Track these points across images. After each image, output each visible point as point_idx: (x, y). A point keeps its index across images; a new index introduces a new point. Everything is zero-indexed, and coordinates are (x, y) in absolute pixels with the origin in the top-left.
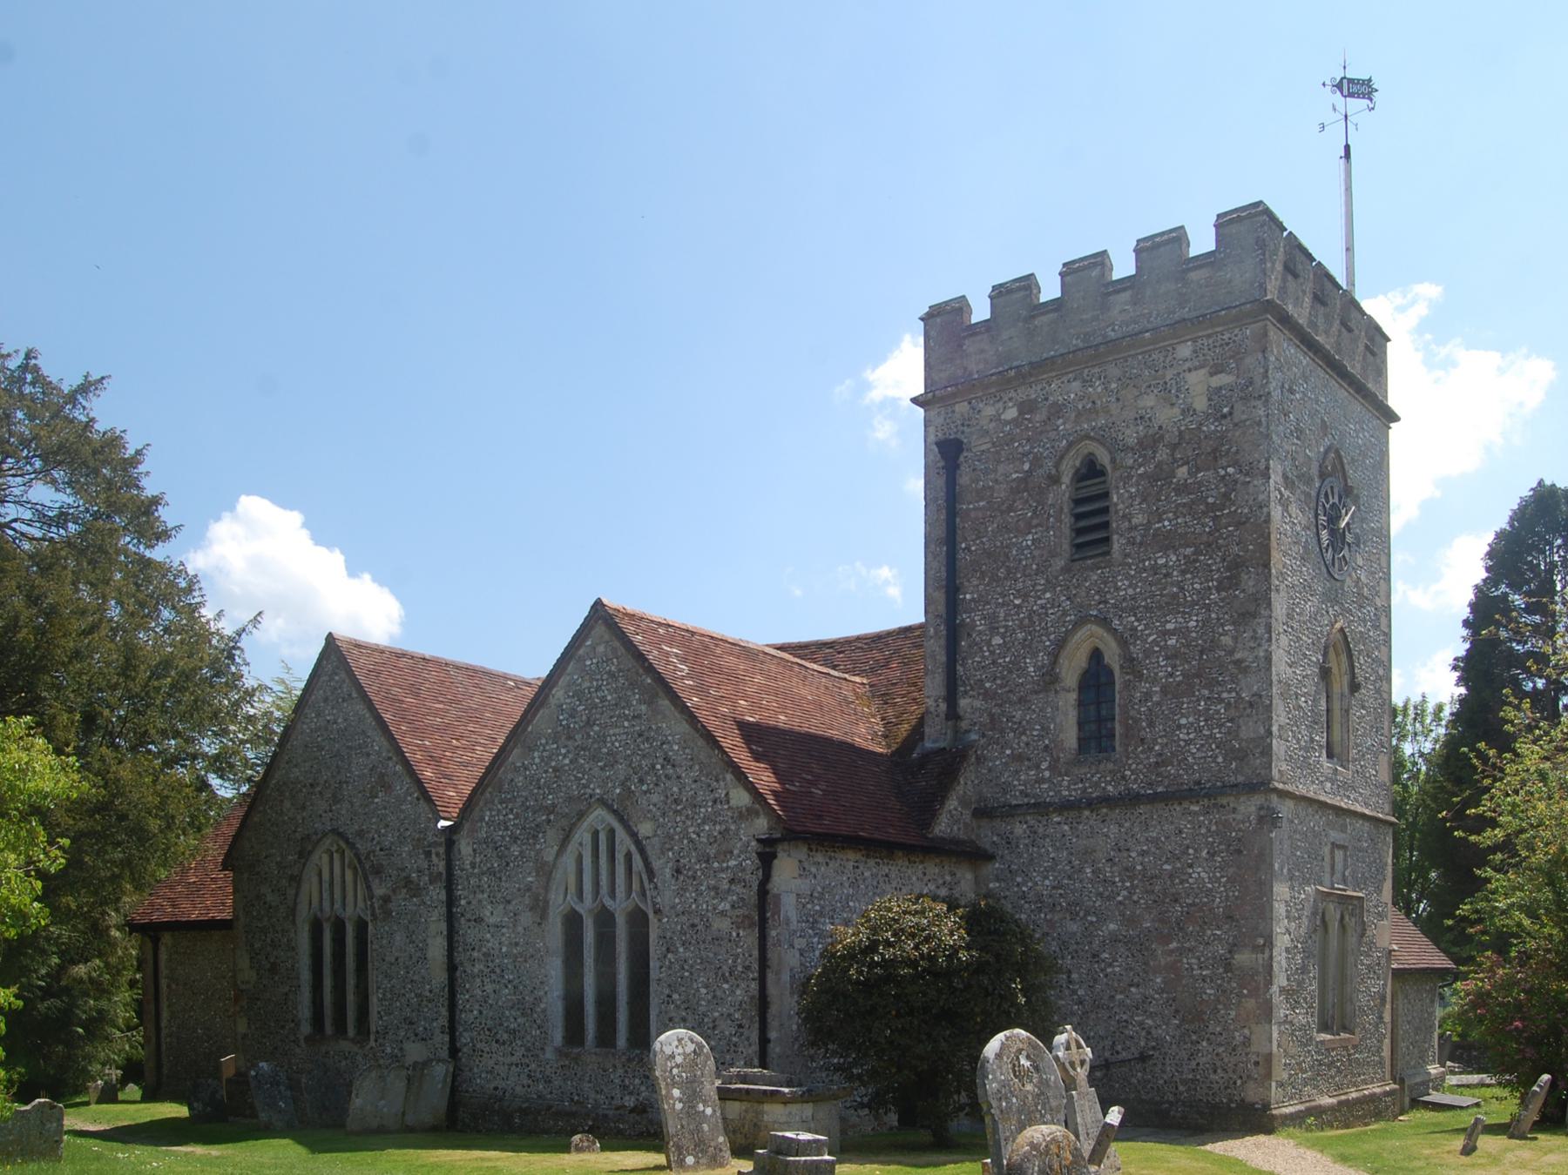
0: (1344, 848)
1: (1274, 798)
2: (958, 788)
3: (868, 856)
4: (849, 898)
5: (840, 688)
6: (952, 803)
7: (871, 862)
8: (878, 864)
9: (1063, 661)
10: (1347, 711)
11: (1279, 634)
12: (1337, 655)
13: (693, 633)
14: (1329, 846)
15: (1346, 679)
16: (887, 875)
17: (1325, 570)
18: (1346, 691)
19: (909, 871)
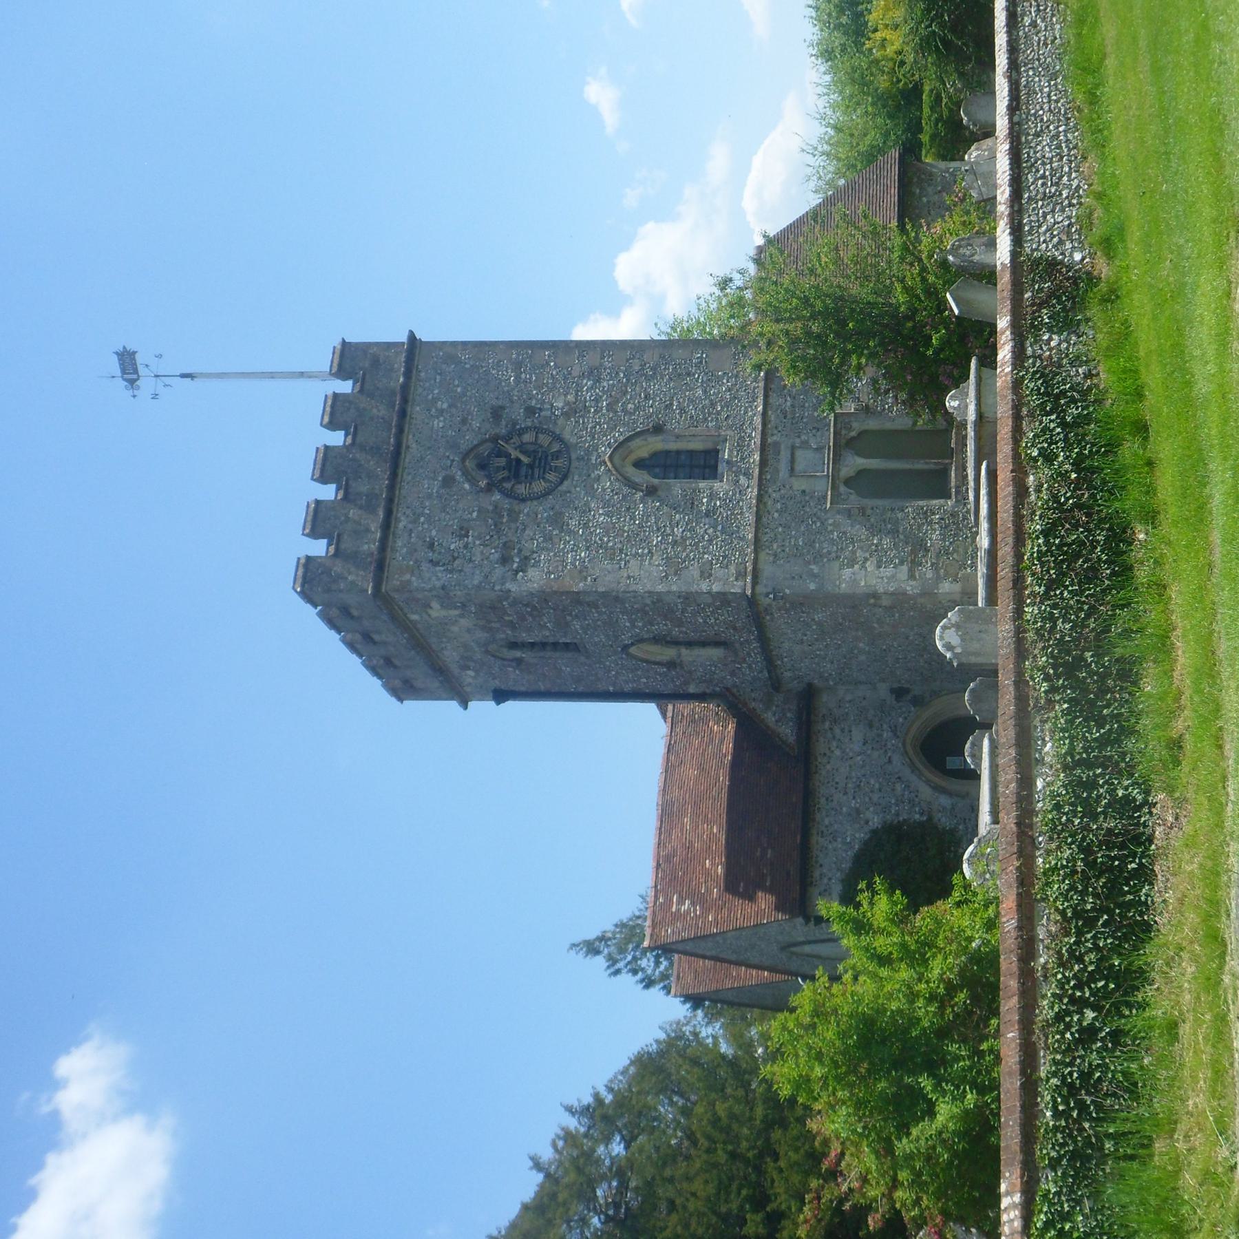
0: (793, 448)
1: (760, 589)
2: (758, 711)
3: (814, 820)
4: (844, 843)
5: (683, 715)
6: (770, 718)
7: (818, 816)
8: (819, 809)
9: (658, 658)
10: (678, 437)
11: (629, 577)
12: (631, 452)
13: (658, 866)
14: (793, 480)
15: (651, 439)
16: (827, 799)
17: (566, 483)
18: (660, 438)
19: (824, 773)
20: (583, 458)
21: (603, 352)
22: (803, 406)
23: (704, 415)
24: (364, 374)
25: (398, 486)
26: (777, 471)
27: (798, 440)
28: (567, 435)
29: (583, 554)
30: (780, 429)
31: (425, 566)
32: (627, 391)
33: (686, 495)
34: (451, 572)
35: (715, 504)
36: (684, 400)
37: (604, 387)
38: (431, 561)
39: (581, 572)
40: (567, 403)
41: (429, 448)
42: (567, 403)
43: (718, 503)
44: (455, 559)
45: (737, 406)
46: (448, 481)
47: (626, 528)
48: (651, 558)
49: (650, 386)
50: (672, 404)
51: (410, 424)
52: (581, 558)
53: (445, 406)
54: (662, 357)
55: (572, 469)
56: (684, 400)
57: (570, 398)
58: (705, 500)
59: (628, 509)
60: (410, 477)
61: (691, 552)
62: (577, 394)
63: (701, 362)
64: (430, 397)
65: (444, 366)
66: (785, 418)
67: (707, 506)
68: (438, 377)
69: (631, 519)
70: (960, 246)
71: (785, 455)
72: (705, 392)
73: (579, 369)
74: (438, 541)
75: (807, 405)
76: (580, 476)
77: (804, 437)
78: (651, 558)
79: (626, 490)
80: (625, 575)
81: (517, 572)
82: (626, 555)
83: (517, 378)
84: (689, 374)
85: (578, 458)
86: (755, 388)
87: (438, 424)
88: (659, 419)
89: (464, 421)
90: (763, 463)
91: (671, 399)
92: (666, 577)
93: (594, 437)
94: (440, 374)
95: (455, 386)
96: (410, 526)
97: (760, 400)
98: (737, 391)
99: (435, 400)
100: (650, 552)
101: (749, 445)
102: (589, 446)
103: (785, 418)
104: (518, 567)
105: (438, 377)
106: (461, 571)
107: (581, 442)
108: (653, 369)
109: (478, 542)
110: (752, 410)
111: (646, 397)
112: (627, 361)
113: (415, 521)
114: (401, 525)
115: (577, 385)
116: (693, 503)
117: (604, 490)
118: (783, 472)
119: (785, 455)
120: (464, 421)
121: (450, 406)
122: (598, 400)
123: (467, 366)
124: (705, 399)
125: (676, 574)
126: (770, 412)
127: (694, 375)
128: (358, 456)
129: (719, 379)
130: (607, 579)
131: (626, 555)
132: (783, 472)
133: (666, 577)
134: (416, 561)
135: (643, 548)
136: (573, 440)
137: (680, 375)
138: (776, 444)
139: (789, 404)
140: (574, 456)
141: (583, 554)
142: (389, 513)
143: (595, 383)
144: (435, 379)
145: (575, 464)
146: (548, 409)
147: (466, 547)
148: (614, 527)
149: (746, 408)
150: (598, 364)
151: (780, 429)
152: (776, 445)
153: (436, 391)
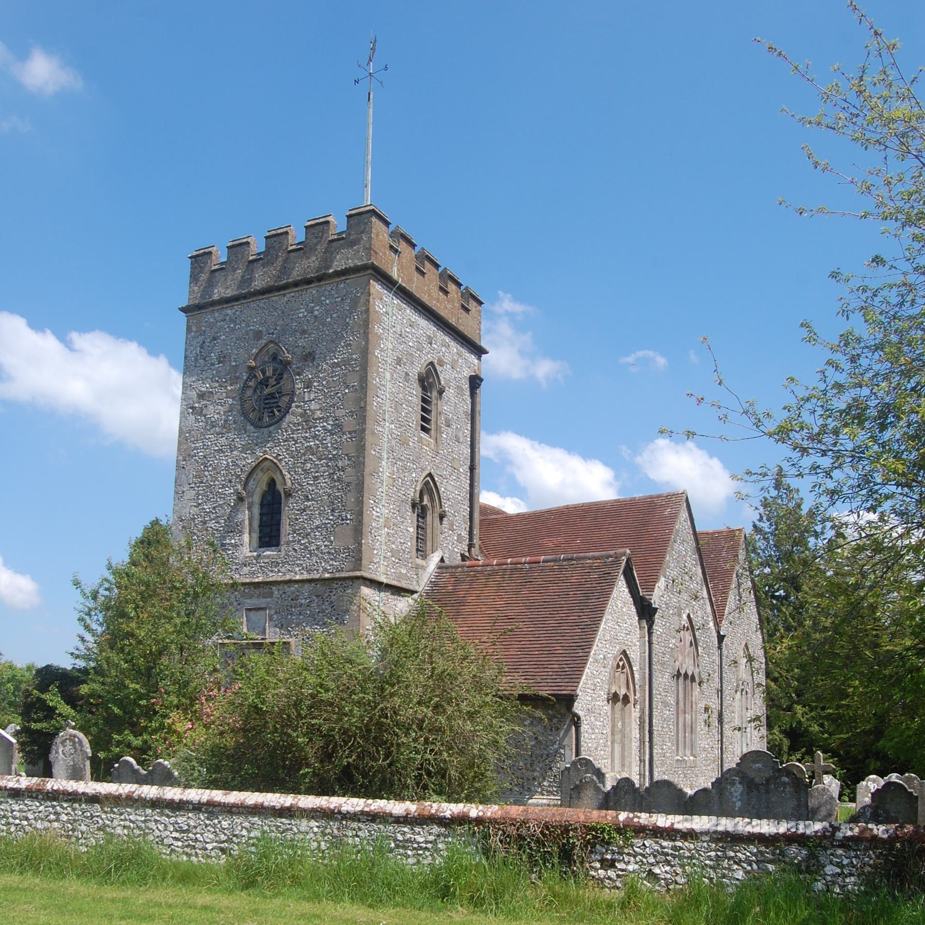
20: (270, 437)
21: (355, 432)
22: (300, 614)
23: (299, 530)
24: (343, 238)
25: (255, 299)
26: (251, 597)
27: (273, 612)
28: (289, 418)
29: (201, 454)
30: (283, 596)
31: (201, 338)
32: (320, 459)
33: (237, 526)
34: (196, 360)
35: (230, 550)
36: (311, 510)
37: (325, 440)
38: (204, 342)
39: (189, 455)
40: (313, 412)
41: (283, 312)
42: (313, 412)
43: (230, 552)
44: (204, 359)
45: (304, 557)
46: (258, 335)
47: (217, 482)
48: (195, 506)
49: (324, 479)
50: (309, 500)
51: (302, 290)
52: (198, 453)
53: (316, 313)
54: (348, 484)
55: (262, 429)
56: (311, 510)
57: (318, 414)
58: (233, 541)
59: (230, 481)
60: (262, 305)
61: (198, 537)
62: (321, 418)
63: (343, 520)
64: (323, 298)
65: (349, 301)
66: (292, 600)
67: (229, 544)
68: (339, 299)
69: (223, 485)
70: (74, 743)
71: (262, 602)
72: (317, 527)
73: (341, 415)
74: (218, 343)
75: (301, 617)
76: (257, 437)
77: (275, 616)
78: (195, 506)
79: (243, 477)
80: (185, 489)
81: (192, 408)
82: (198, 487)
83: (338, 365)
84: (333, 511)
85: (270, 432)
86: (317, 570)
87: (302, 313)
88: (297, 492)
89: (304, 332)
90: (257, 585)
91: (313, 499)
92: (182, 520)
93: (286, 441)
94: (342, 299)
95: (331, 316)
96: (228, 318)
97: (306, 576)
98: (317, 556)
99: (320, 303)
100: (199, 504)
101: (272, 571)
102: (278, 439)
103: (292, 600)
104: (196, 407)
105: (339, 299)
106: (196, 366)
107: (282, 431)
108: (339, 480)
109: (214, 372)
110: (300, 570)
111: (316, 477)
112: (347, 455)
113: (231, 321)
114: (229, 312)
115: (328, 417)
116: (232, 532)
117: (245, 458)
118: (250, 603)
119: (262, 602)
120: (304, 332)
121: (316, 316)
122: (315, 437)
123: (348, 320)
124: (311, 528)
125: (183, 527)
126: (296, 586)
127: (332, 515)
128: (280, 259)
129: (326, 538)
130: (183, 476)
131: (198, 487)
132: (250, 603)
133: (182, 520)
134: (204, 332)
135: (202, 499)
136: (284, 425)
137: (333, 503)
138: (271, 595)
139: (303, 601)
140: (271, 428)
141: (201, 454)
142: (245, 297)
143: (329, 431)
144: (338, 297)
145: (266, 430)
146: (310, 397)
147: (213, 364)
148: (218, 473)
149: (302, 565)
150: (344, 430)
151: (283, 596)
152: (271, 595)
153: (328, 302)
